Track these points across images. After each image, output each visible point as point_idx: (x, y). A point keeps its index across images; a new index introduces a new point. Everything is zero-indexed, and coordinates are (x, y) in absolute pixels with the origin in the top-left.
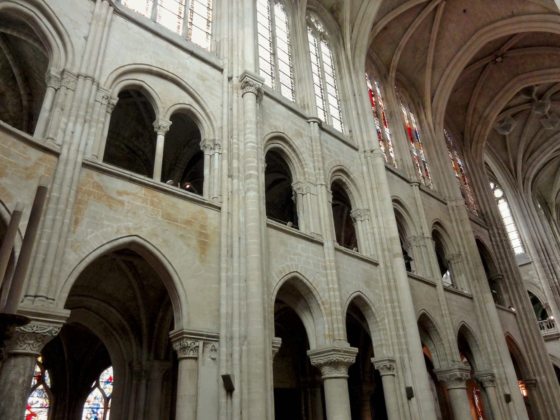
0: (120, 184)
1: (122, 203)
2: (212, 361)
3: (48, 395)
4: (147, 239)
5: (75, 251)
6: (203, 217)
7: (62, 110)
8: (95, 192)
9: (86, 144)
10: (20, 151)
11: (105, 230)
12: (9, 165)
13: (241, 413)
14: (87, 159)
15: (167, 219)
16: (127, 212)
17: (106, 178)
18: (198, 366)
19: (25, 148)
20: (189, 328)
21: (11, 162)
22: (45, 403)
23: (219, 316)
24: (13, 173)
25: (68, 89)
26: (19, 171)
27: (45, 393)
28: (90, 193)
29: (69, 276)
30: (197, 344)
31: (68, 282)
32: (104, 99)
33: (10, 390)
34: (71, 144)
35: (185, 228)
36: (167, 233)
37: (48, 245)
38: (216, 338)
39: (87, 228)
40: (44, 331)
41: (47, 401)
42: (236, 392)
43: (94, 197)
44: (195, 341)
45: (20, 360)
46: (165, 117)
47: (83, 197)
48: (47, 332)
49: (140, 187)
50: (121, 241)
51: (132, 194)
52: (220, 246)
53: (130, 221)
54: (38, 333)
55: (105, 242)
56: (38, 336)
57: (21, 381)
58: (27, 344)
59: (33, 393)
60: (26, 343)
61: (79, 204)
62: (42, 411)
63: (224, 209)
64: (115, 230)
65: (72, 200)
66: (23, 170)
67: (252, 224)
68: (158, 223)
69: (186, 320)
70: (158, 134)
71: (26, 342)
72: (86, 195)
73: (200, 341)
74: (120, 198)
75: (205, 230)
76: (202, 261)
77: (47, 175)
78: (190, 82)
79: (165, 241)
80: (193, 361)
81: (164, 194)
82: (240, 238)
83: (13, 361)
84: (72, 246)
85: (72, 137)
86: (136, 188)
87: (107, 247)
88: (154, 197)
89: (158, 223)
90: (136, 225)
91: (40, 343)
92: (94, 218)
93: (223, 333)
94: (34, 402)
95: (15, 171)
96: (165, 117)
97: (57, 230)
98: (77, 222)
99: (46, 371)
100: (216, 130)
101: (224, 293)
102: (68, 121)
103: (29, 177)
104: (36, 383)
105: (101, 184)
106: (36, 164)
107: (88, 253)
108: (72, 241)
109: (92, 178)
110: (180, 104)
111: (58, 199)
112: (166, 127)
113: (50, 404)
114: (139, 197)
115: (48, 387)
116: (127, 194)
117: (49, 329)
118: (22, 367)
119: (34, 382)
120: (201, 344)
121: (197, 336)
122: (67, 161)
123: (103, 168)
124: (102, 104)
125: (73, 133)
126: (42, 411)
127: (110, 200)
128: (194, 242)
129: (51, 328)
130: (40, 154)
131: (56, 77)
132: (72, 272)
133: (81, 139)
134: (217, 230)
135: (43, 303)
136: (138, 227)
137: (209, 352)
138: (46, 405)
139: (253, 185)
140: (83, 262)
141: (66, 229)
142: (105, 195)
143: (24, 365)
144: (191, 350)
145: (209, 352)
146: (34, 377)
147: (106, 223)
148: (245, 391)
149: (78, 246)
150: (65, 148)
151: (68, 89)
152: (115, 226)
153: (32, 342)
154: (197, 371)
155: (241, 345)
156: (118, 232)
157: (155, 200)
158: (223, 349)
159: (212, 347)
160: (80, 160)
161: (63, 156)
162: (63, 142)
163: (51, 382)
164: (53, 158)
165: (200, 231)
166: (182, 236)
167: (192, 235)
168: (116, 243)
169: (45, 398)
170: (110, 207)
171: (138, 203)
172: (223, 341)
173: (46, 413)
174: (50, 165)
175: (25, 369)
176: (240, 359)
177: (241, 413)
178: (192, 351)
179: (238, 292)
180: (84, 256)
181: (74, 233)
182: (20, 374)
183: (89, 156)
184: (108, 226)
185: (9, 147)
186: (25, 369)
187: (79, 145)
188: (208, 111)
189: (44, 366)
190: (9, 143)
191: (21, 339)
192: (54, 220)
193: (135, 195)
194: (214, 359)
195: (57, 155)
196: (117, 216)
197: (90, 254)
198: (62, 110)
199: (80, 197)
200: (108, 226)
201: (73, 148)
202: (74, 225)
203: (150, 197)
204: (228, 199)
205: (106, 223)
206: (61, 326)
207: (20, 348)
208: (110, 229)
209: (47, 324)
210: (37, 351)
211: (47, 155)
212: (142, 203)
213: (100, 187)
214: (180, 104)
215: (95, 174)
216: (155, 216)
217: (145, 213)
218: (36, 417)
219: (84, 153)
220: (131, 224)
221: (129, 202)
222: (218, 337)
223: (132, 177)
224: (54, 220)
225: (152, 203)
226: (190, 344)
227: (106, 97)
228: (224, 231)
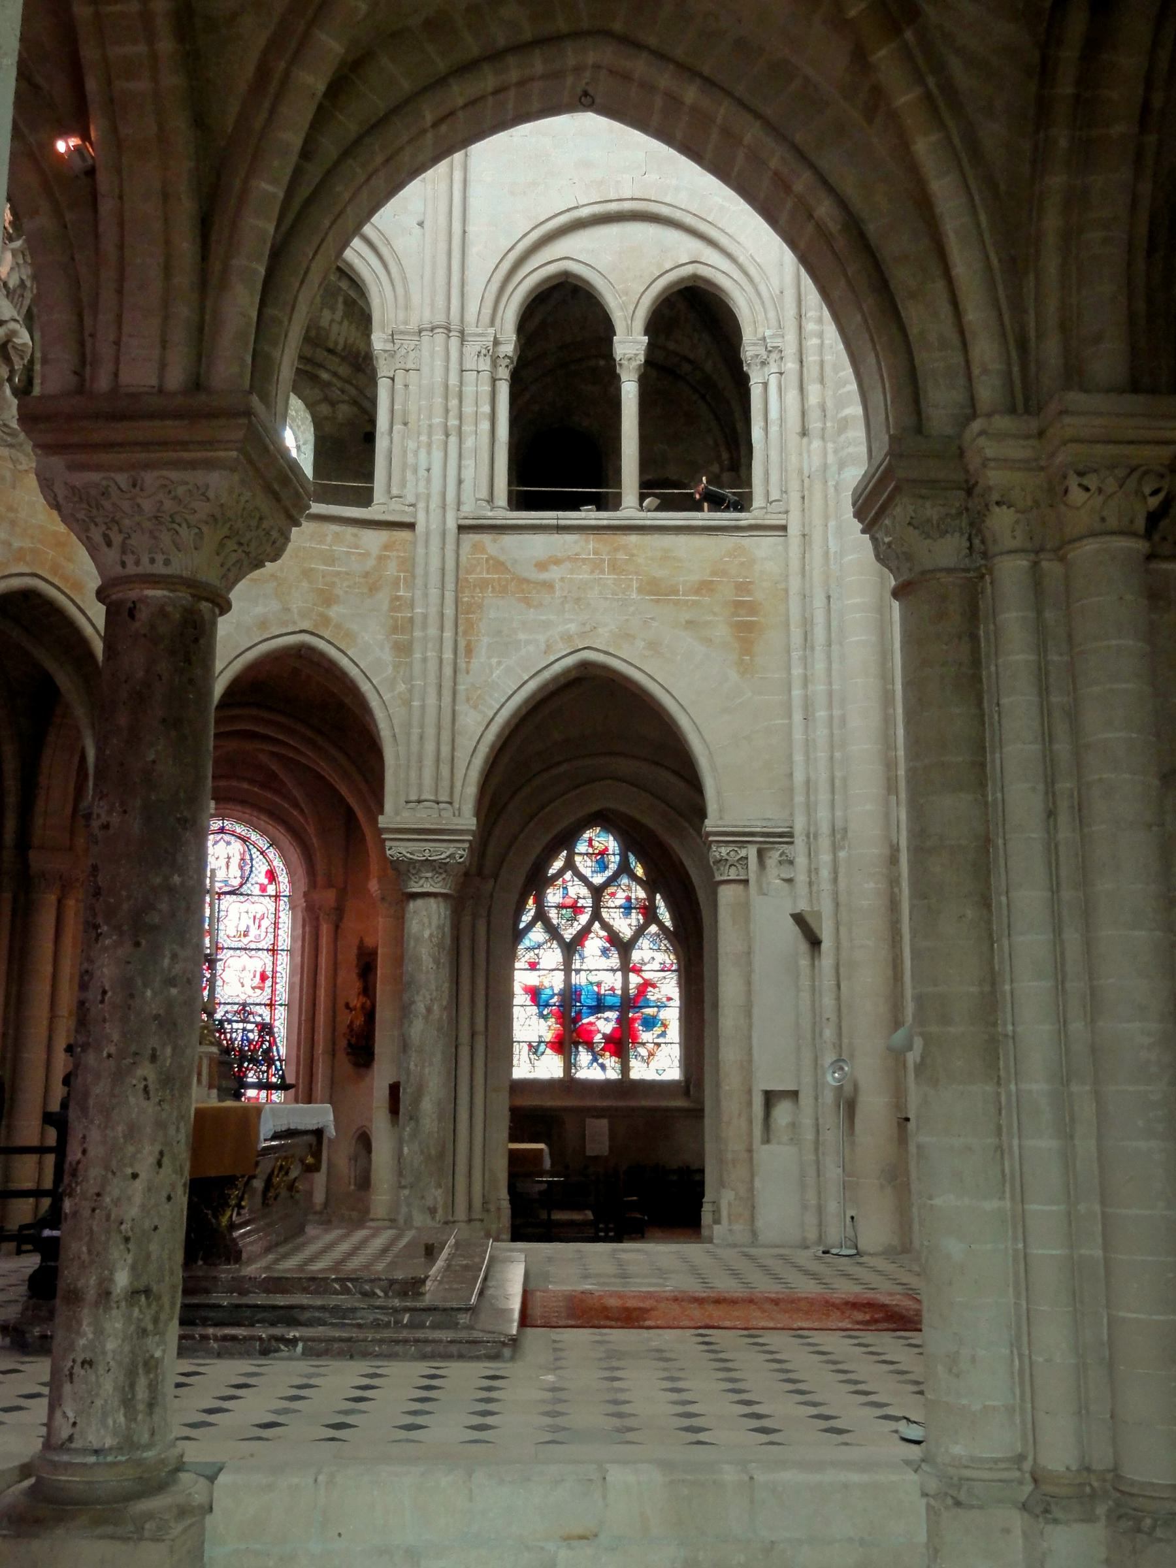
0: (539, 545)
1: (549, 586)
2: (785, 885)
3: (672, 945)
4: (611, 650)
5: (475, 707)
6: (742, 564)
7: (405, 424)
8: (494, 579)
9: (460, 482)
10: (348, 547)
11: (523, 652)
12: (336, 580)
13: (838, 986)
14: (466, 515)
15: (651, 593)
16: (562, 603)
17: (509, 540)
18: (748, 896)
19: (355, 535)
20: (720, 823)
21: (338, 573)
22: (668, 961)
23: (791, 790)
24: (346, 592)
25: (407, 371)
26: (355, 583)
27: (666, 942)
28: (483, 584)
29: (472, 755)
30: (743, 853)
31: (472, 767)
32: (481, 358)
33: (415, 947)
34: (429, 496)
35: (695, 603)
36: (655, 624)
37: (423, 707)
38: (787, 837)
39: (489, 658)
40: (442, 857)
41: (672, 957)
42: (827, 945)
43: (493, 592)
44: (740, 848)
45: (420, 902)
46: (629, 331)
47: (473, 597)
48: (448, 857)
49: (584, 537)
50: (557, 668)
51: (569, 558)
52: (787, 625)
53: (571, 621)
54: (435, 861)
55: (526, 678)
56: (437, 865)
57: (427, 934)
58: (424, 879)
59: (640, 941)
60: (421, 878)
61: (467, 614)
62: (665, 978)
63: (794, 530)
64: (543, 647)
65: (449, 612)
66: (362, 580)
67: (850, 558)
68: (632, 609)
69: (715, 806)
70: (623, 380)
71: (423, 875)
72: (478, 590)
73: (749, 846)
74: (545, 576)
75: (749, 592)
76: (745, 669)
77: (402, 575)
78: (682, 200)
79: (653, 646)
80: (740, 888)
81: (639, 537)
82: (829, 598)
83: (412, 905)
84: (468, 700)
85: (428, 481)
86: (576, 542)
87: (532, 686)
88: (616, 550)
89: (632, 609)
90: (584, 624)
91: (444, 876)
92: (499, 633)
93: (799, 826)
94: (646, 961)
95: (349, 587)
96: (629, 331)
97: (432, 678)
98: (469, 651)
99: (658, 897)
100: (769, 304)
101: (798, 736)
102: (419, 447)
103: (373, 589)
104: (641, 922)
105: (502, 558)
106: (381, 558)
107: (498, 707)
108: (467, 690)
109: (483, 550)
110: (667, 272)
111: (425, 616)
112: (636, 355)
113: (679, 963)
114: (584, 560)
115: (667, 928)
116: (557, 562)
117: (448, 854)
118: (425, 913)
119: (638, 920)
120: (752, 852)
121: (740, 838)
122: (428, 534)
123: (499, 522)
124: (478, 372)
125: (428, 470)
126: (665, 978)
127: (524, 586)
128: (721, 631)
129: (451, 850)
130: (383, 536)
131: (385, 351)
132: (476, 747)
133: (445, 476)
134: (783, 586)
135: (429, 812)
136: (588, 628)
137: (776, 866)
138: (672, 964)
139: (851, 450)
140: (492, 724)
141: (448, 671)
142: (513, 579)
143: (426, 910)
144: (731, 866)
145: (776, 866)
146: (635, 908)
147: (522, 636)
148: (845, 943)
149: (479, 697)
150: (421, 505)
151: (407, 371)
152: (541, 638)
153: (429, 875)
154: (745, 908)
155: (835, 849)
156: (548, 649)
157: (621, 556)
158: (801, 861)
159: (781, 855)
160: (451, 525)
161: (420, 528)
162: (417, 496)
163: (673, 919)
164: (405, 534)
165: (734, 601)
166: (690, 624)
167: (715, 614)
168: (547, 675)
169: (665, 951)
170: (527, 601)
171: (584, 576)
172: (799, 841)
173: (674, 982)
174: (405, 552)
175: (429, 917)
176: (835, 880)
177: (838, 986)
178: (733, 867)
179: (826, 731)
180: (491, 714)
181: (468, 672)
182: (424, 924)
183: (468, 508)
184: (528, 642)
185: (330, 546)
186: (429, 917)
187: (444, 495)
188: (741, 259)
189: (651, 885)
190: (329, 539)
191: (414, 872)
192: (425, 660)
193: (574, 559)
194: (790, 881)
195: (411, 526)
196: (543, 618)
197: (503, 705)
198: (405, 424)
199: (466, 599)
200: (528, 642)
201: (435, 503)
202: (466, 656)
203: (608, 554)
204: (803, 498)
205: (522, 636)
206: (467, 845)
207: (416, 885)
208: (531, 648)
209: (445, 845)
210: (441, 887)
211: (395, 533)
212: (592, 572)
213: (502, 564)
214: (667, 272)
215: (486, 538)
216: (624, 593)
217: (601, 593)
218: (657, 989)
219: (459, 503)
220: (573, 627)
221: (562, 579)
222: (791, 835)
223: (562, 522)
224: (425, 660)
225: (614, 567)
226: (728, 854)
227: (484, 351)
228: (795, 584)
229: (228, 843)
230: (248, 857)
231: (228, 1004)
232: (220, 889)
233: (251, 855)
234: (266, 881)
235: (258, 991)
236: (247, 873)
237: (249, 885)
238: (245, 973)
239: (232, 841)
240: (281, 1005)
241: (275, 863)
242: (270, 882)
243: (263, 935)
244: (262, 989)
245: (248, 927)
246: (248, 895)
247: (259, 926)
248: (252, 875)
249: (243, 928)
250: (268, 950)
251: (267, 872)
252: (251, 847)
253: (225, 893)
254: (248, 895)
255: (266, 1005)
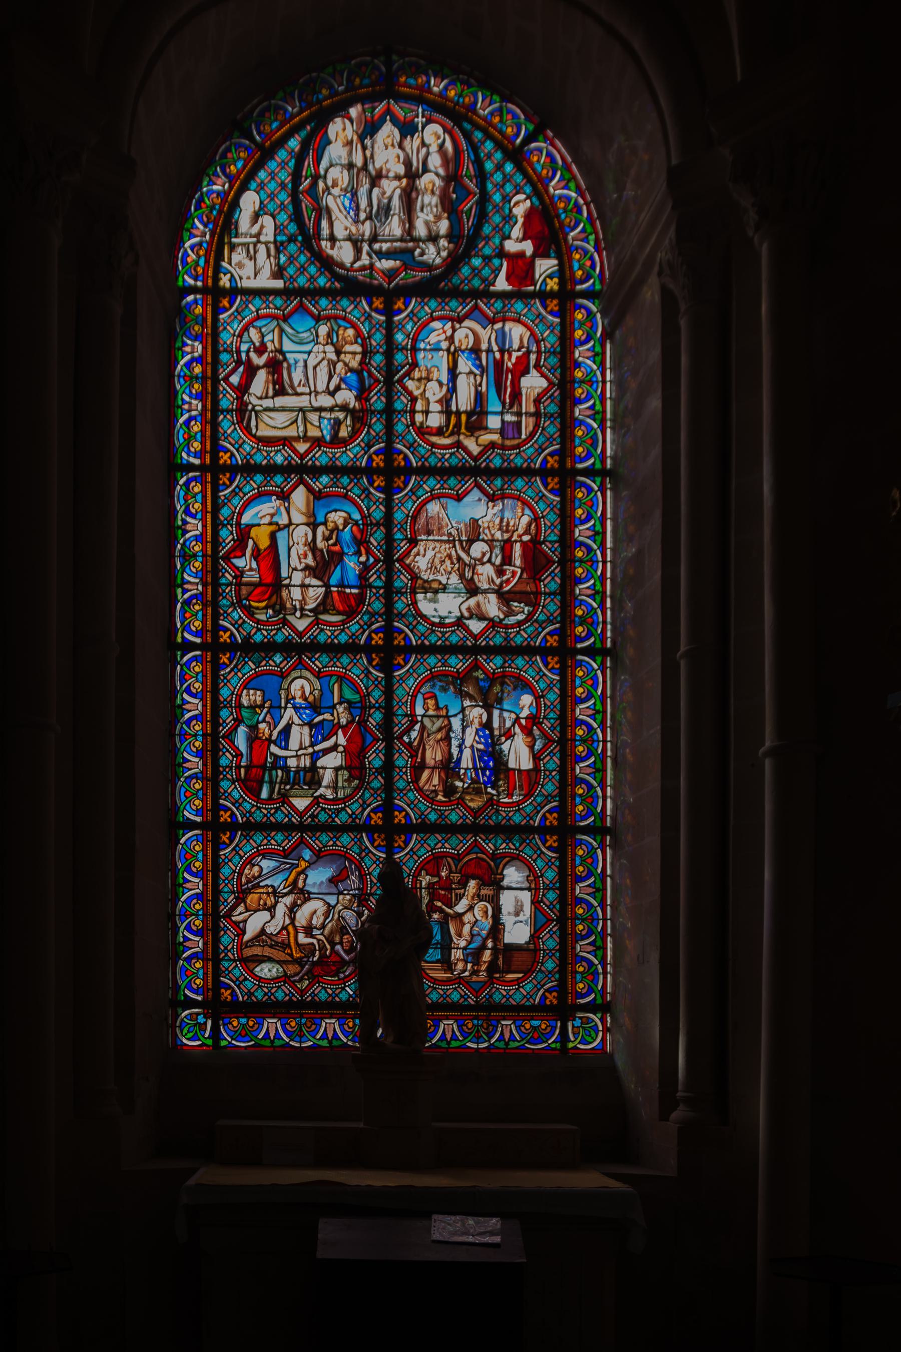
229: (407, 129)
230: (468, 168)
231: (433, 649)
232: (391, 275)
233: (479, 163)
234: (528, 247)
235: (521, 611)
236: (468, 224)
237: (477, 262)
238: (478, 549)
239: (420, 120)
240: (590, 652)
241: (555, 189)
242: (541, 252)
243: (527, 424)
244: (532, 599)
245: (480, 398)
246: (475, 294)
247: (516, 395)
248: (487, 230)
249: (464, 399)
250: (544, 473)
251: (529, 216)
252: (478, 135)
253: (408, 292)
254: (475, 294)
255: (544, 652)
